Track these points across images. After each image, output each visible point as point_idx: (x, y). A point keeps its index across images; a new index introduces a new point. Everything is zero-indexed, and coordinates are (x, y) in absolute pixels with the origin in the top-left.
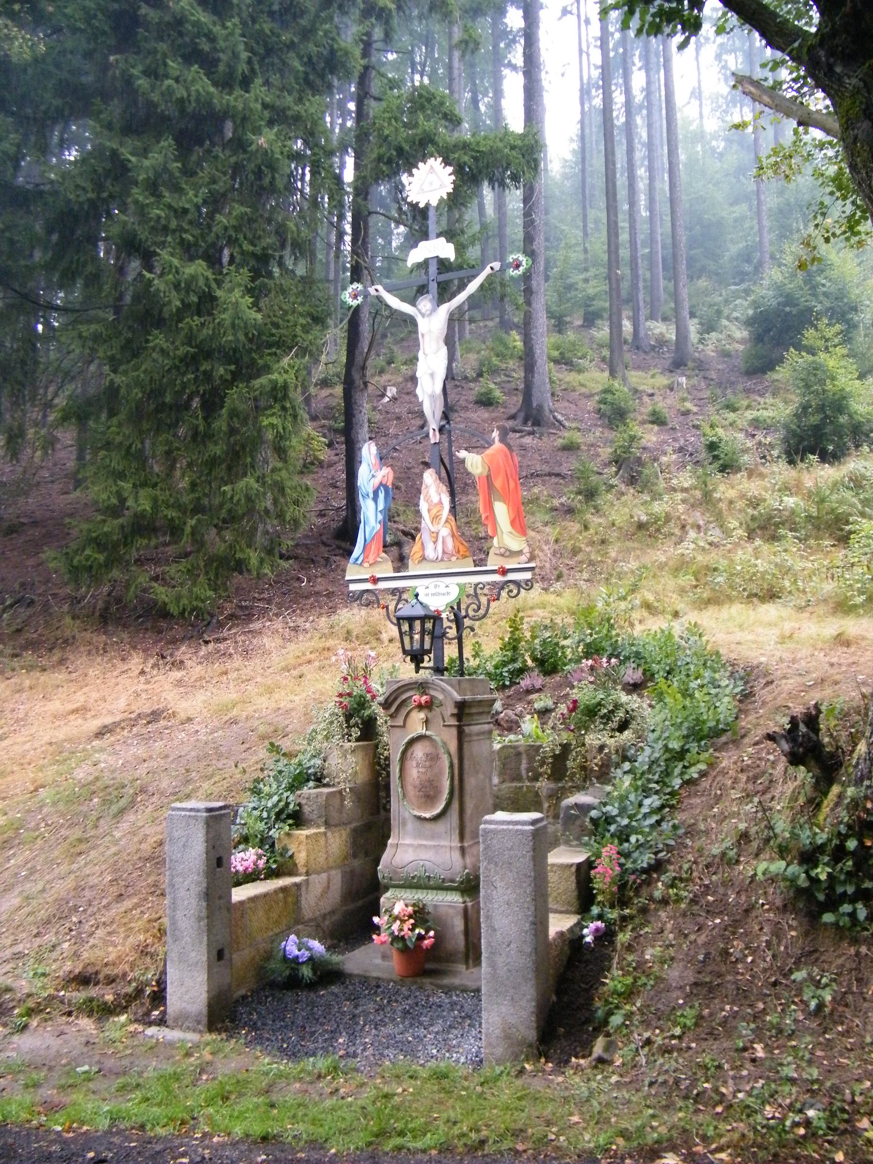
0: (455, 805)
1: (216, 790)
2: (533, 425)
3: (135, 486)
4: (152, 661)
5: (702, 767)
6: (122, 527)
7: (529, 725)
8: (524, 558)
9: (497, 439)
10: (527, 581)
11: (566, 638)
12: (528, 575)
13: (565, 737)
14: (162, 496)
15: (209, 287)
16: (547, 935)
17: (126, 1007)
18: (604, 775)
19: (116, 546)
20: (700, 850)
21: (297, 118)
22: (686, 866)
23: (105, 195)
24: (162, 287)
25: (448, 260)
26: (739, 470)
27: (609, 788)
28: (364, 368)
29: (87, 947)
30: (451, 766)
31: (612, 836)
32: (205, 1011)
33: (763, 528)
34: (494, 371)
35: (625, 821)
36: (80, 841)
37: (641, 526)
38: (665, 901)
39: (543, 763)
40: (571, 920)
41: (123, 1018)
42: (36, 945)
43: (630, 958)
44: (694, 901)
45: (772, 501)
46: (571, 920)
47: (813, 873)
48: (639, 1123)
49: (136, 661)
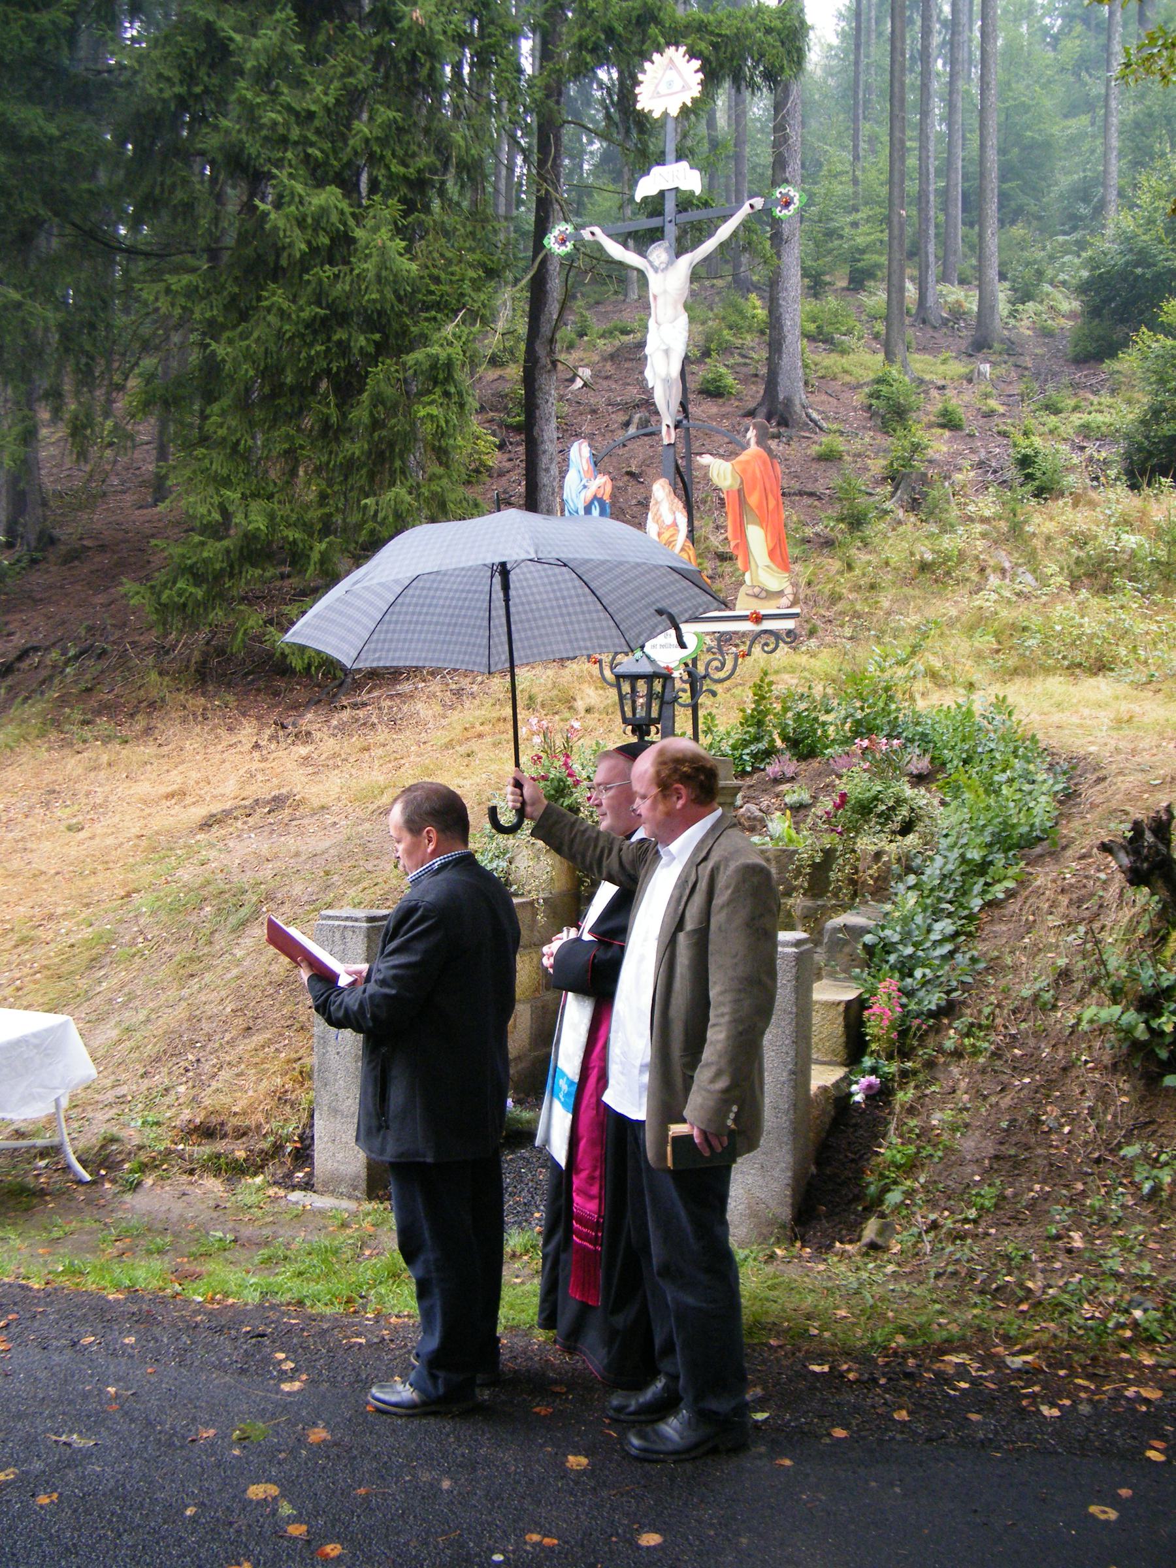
1: (367, 897)
2: (779, 424)
3: (244, 497)
4: (268, 732)
5: (1011, 884)
6: (228, 551)
7: (779, 824)
8: (785, 601)
9: (753, 441)
10: (789, 632)
11: (828, 712)
12: (790, 624)
13: (827, 841)
14: (282, 511)
15: (345, 224)
16: (808, 1090)
17: (262, 1167)
18: (881, 891)
19: (218, 577)
20: (1006, 992)
22: (987, 1011)
24: (281, 223)
25: (692, 193)
26: (1062, 494)
27: (888, 907)
28: (552, 341)
29: (209, 1090)
31: (892, 968)
32: (363, 1174)
33: (1091, 575)
34: (726, 349)
35: (909, 950)
36: (191, 960)
37: (924, 567)
38: (958, 1054)
39: (798, 873)
40: (838, 1073)
41: (259, 1179)
42: (144, 1088)
43: (912, 1123)
44: (996, 1055)
45: (1105, 539)
46: (838, 1073)
47: (1154, 1024)
48: (924, 1319)
49: (247, 732)
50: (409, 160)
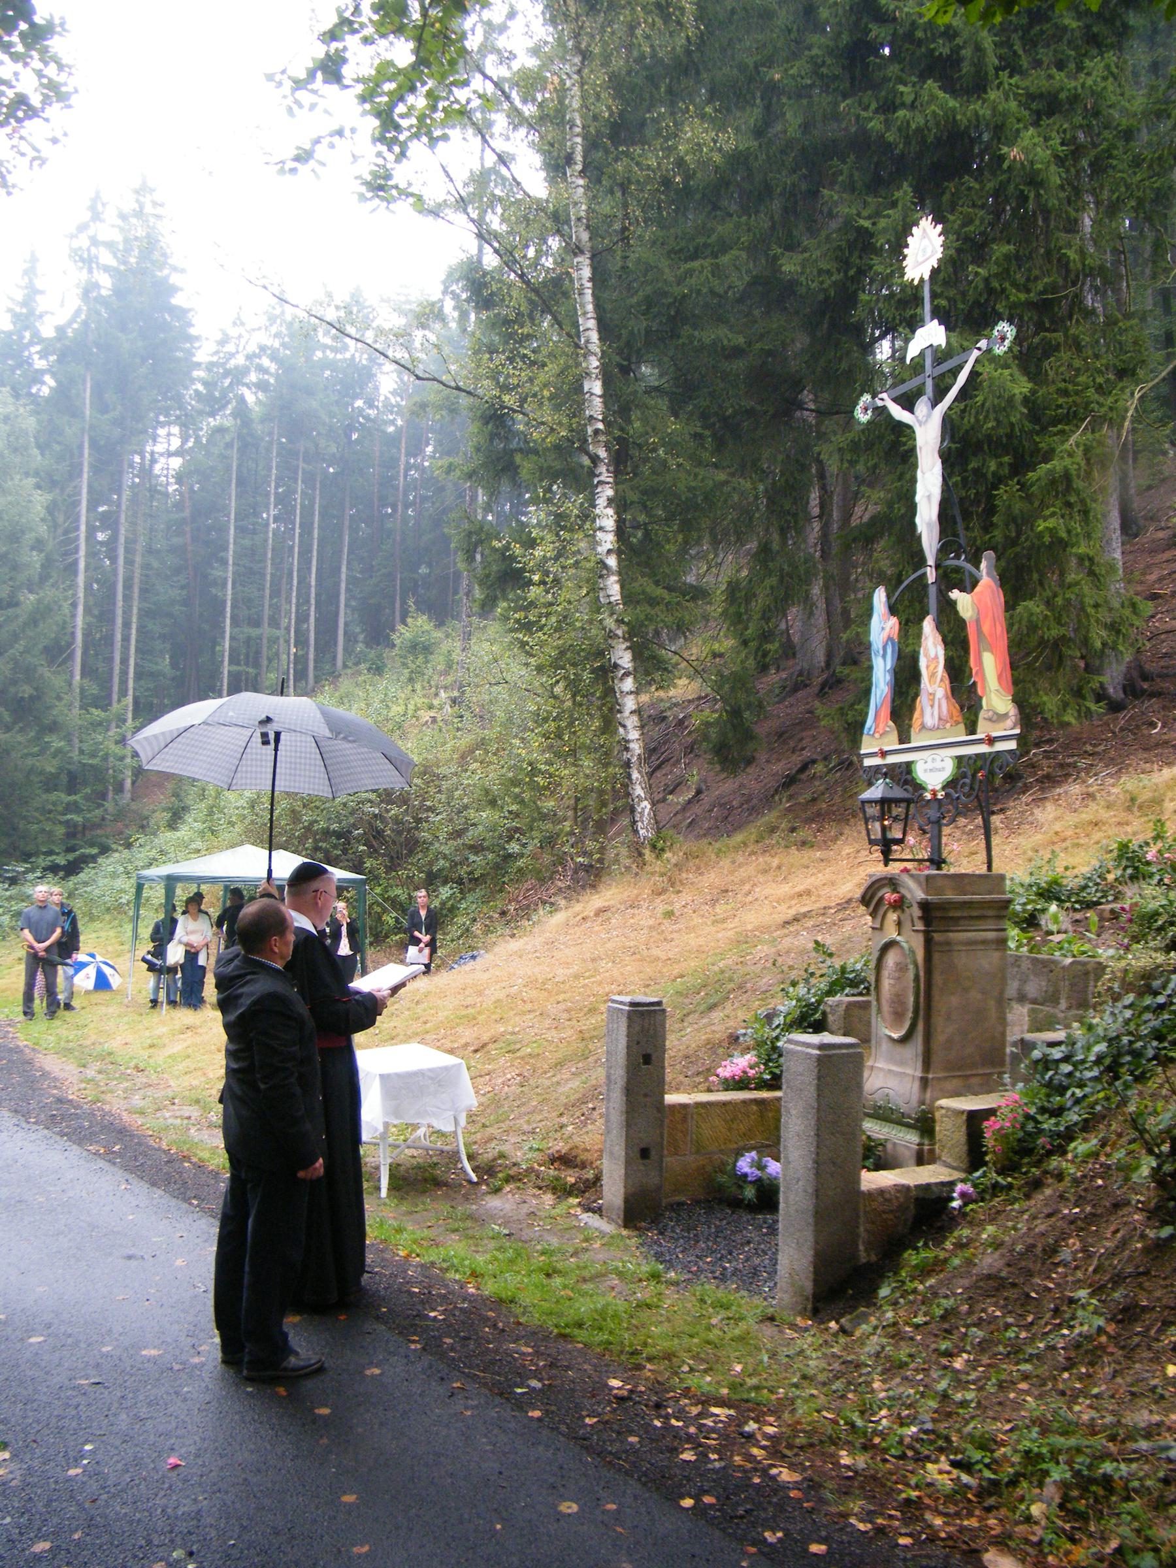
0: (920, 1027)
21: (1075, 99)
23: (851, 273)
30: (917, 979)
50: (1031, 285)
